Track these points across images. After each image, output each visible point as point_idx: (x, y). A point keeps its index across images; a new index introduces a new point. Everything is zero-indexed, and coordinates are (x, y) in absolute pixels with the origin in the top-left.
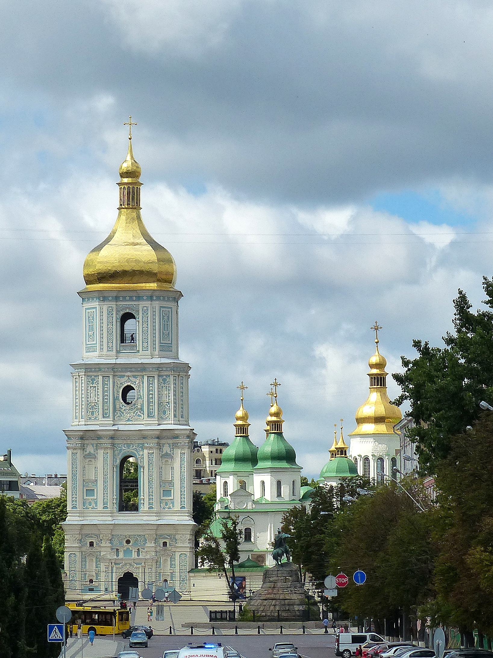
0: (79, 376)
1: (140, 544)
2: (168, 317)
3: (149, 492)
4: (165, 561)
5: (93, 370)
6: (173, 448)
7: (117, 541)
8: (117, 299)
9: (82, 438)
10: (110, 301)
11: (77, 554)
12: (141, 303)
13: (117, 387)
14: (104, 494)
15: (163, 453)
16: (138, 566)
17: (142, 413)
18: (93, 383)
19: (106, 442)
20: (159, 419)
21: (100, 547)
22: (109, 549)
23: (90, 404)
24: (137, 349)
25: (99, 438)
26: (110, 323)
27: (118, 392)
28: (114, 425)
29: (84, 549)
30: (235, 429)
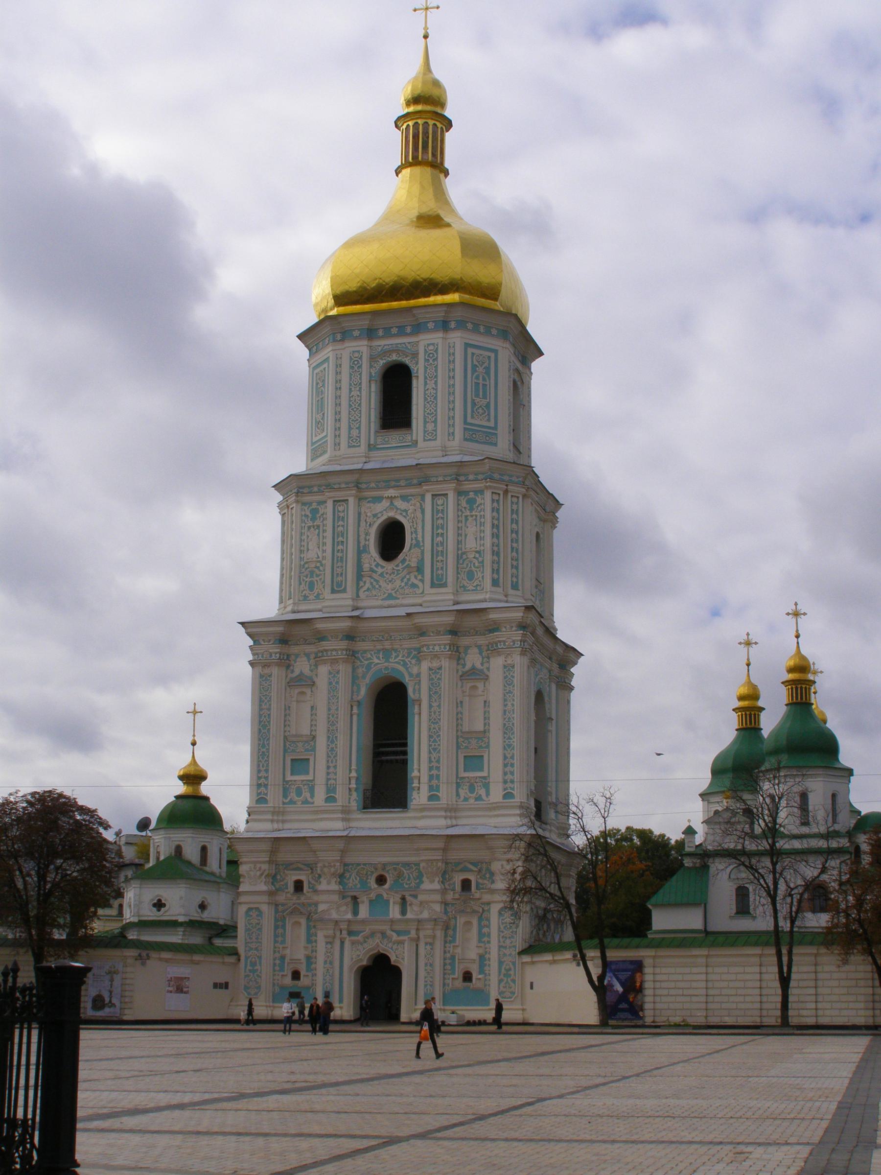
0: (288, 507)
1: (407, 886)
2: (487, 369)
3: (430, 761)
4: (468, 923)
5: (316, 489)
6: (488, 658)
7: (356, 879)
8: (370, 334)
10: (356, 338)
11: (264, 908)
13: (367, 523)
14: (328, 767)
15: (467, 668)
16: (401, 938)
17: (420, 580)
18: (313, 519)
19: (335, 646)
20: (457, 591)
21: (316, 891)
22: (335, 898)
23: (306, 566)
24: (414, 439)
25: (321, 637)
26: (355, 385)
27: (367, 534)
28: (356, 608)
29: (281, 898)
30: (737, 718)
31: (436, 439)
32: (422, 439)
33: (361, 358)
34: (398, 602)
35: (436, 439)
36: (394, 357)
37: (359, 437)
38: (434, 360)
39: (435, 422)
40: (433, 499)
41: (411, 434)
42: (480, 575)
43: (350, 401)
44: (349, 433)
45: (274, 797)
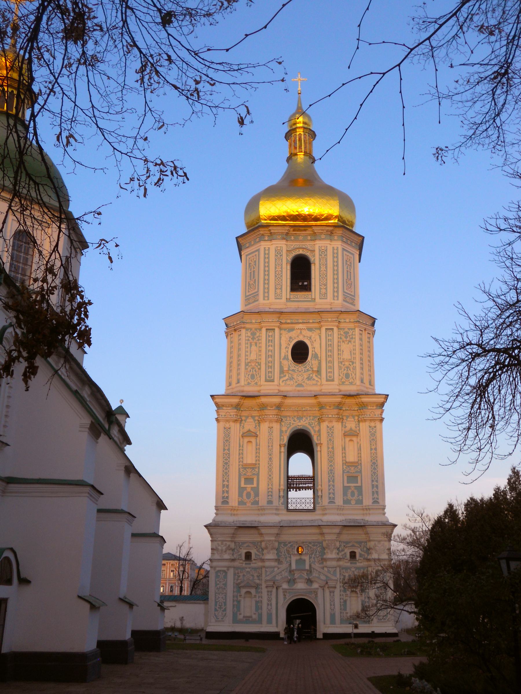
9: (237, 407)
12: (317, 242)
19: (271, 412)
24: (313, 297)
31: (326, 299)
32: (319, 298)
33: (282, 251)
34: (305, 388)
35: (326, 299)
36: (301, 252)
37: (281, 294)
38: (325, 255)
39: (326, 289)
40: (326, 332)
41: (311, 295)
42: (353, 375)
43: (276, 273)
44: (275, 291)
45: (234, 500)
